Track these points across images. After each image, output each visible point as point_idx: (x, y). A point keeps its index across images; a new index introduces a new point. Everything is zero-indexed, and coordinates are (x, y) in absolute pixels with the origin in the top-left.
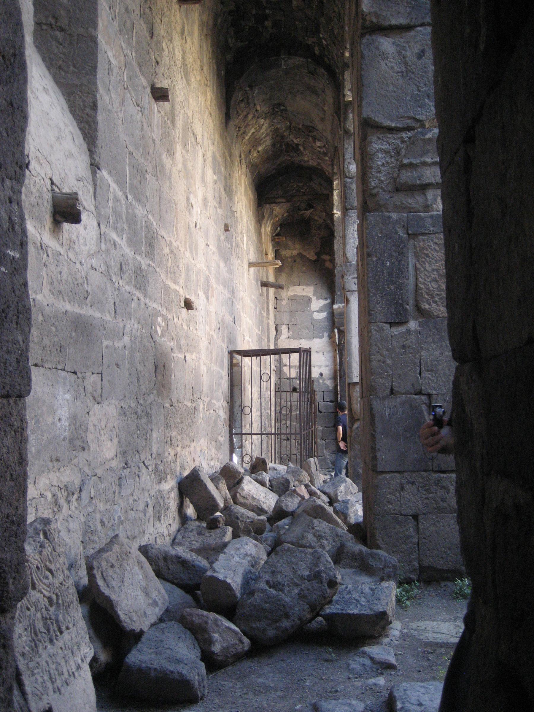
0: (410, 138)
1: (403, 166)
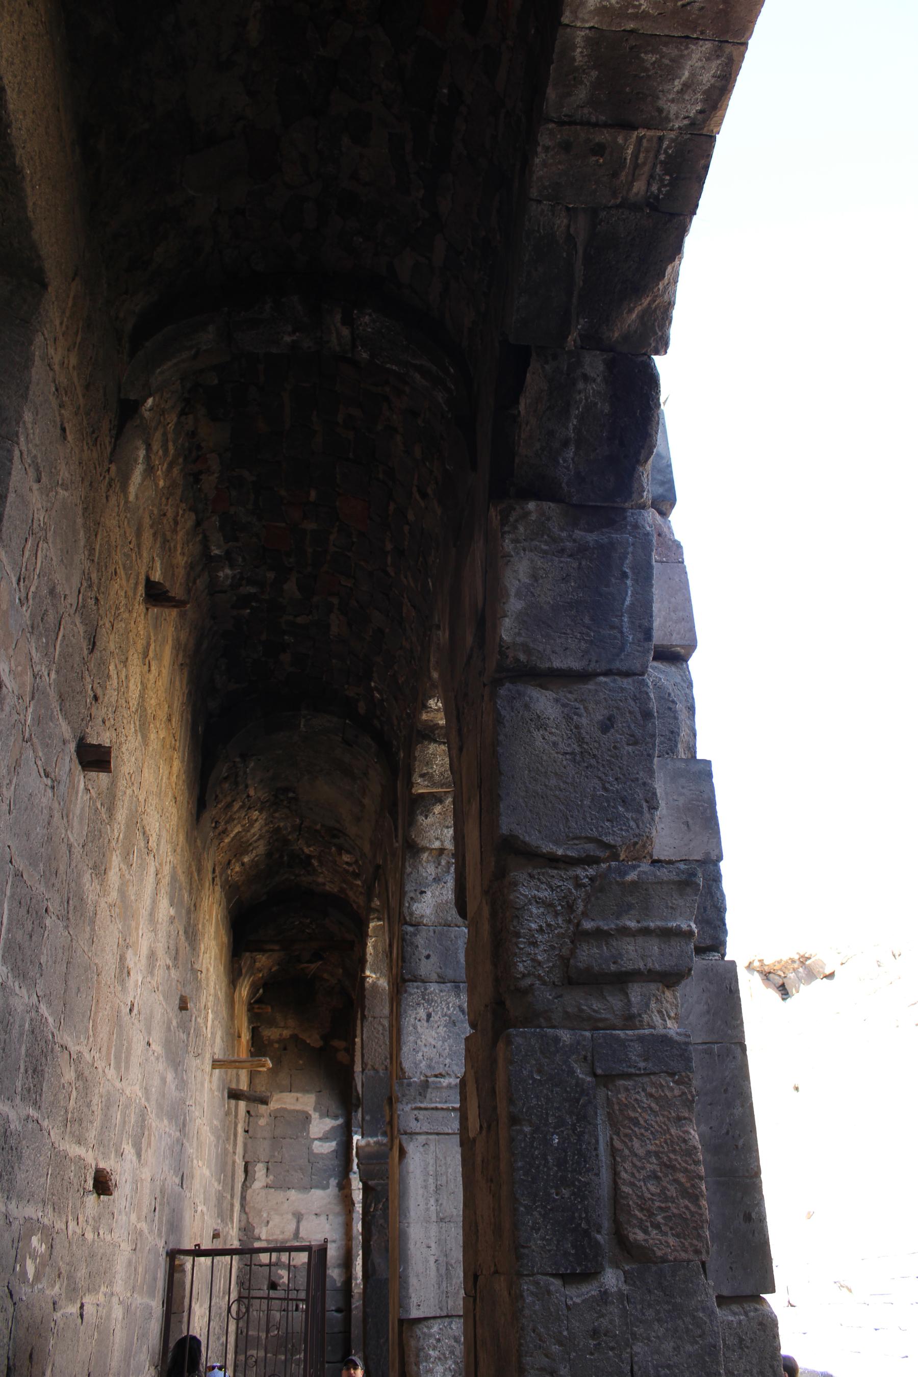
0: (592, 879)
1: (580, 936)
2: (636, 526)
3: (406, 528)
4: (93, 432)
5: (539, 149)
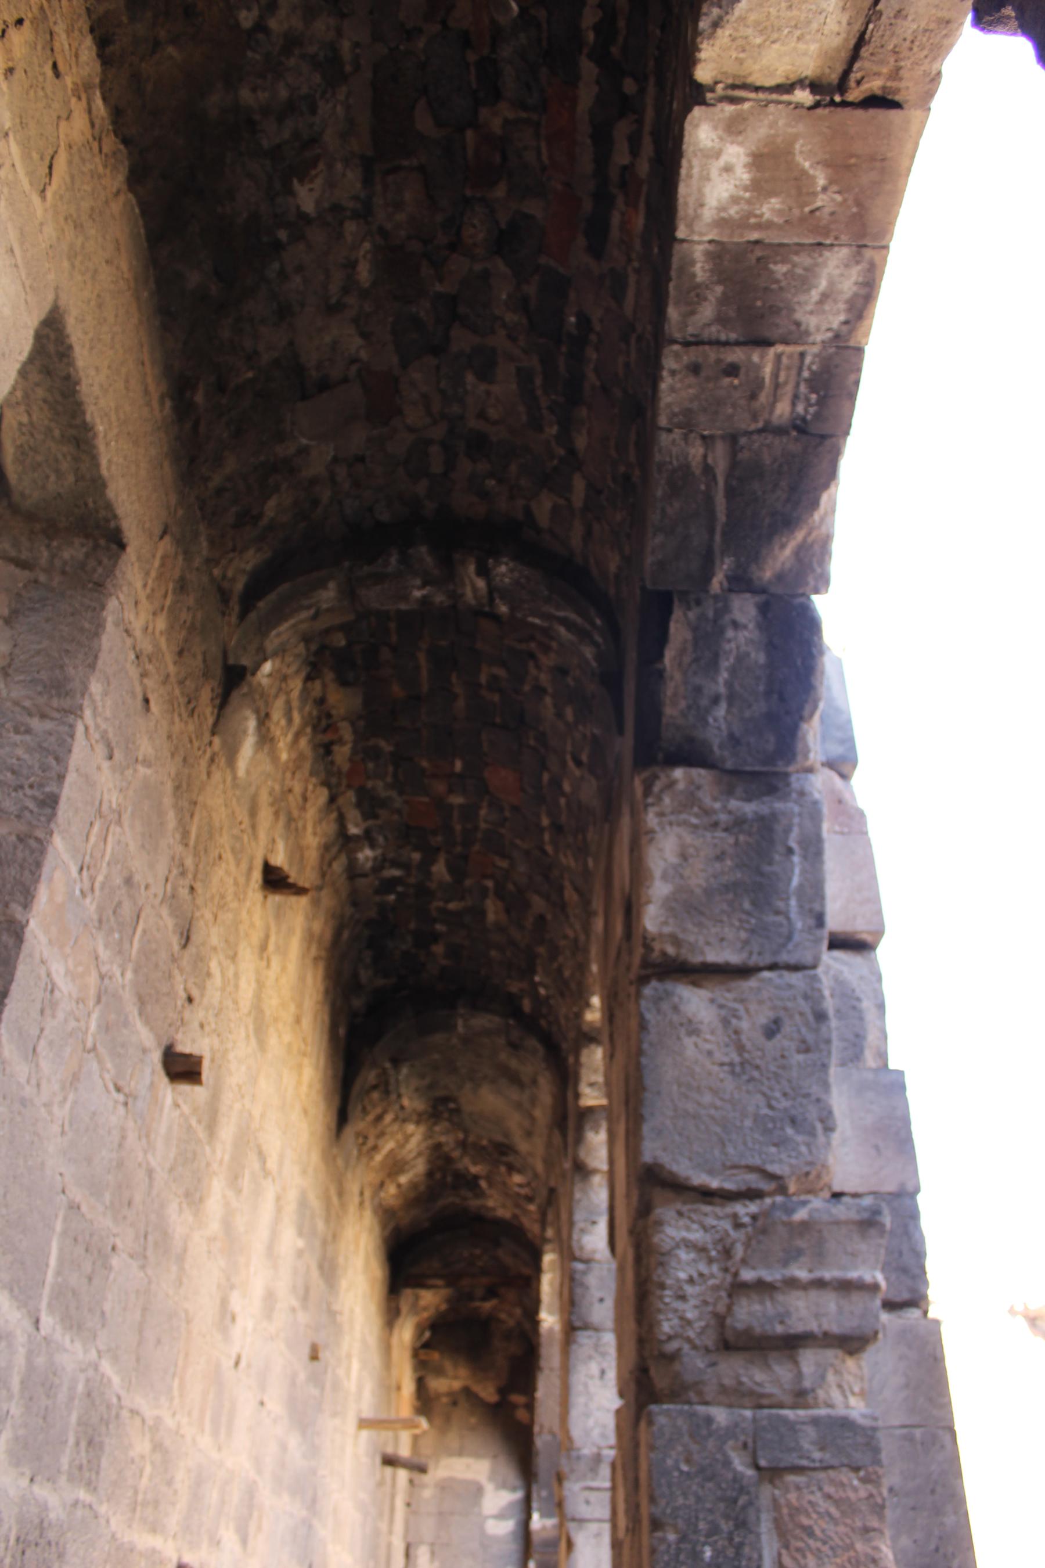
0: (754, 1217)
1: (738, 1288)
2: (802, 793)
3: (563, 801)
4: (189, 702)
5: (665, 373)
